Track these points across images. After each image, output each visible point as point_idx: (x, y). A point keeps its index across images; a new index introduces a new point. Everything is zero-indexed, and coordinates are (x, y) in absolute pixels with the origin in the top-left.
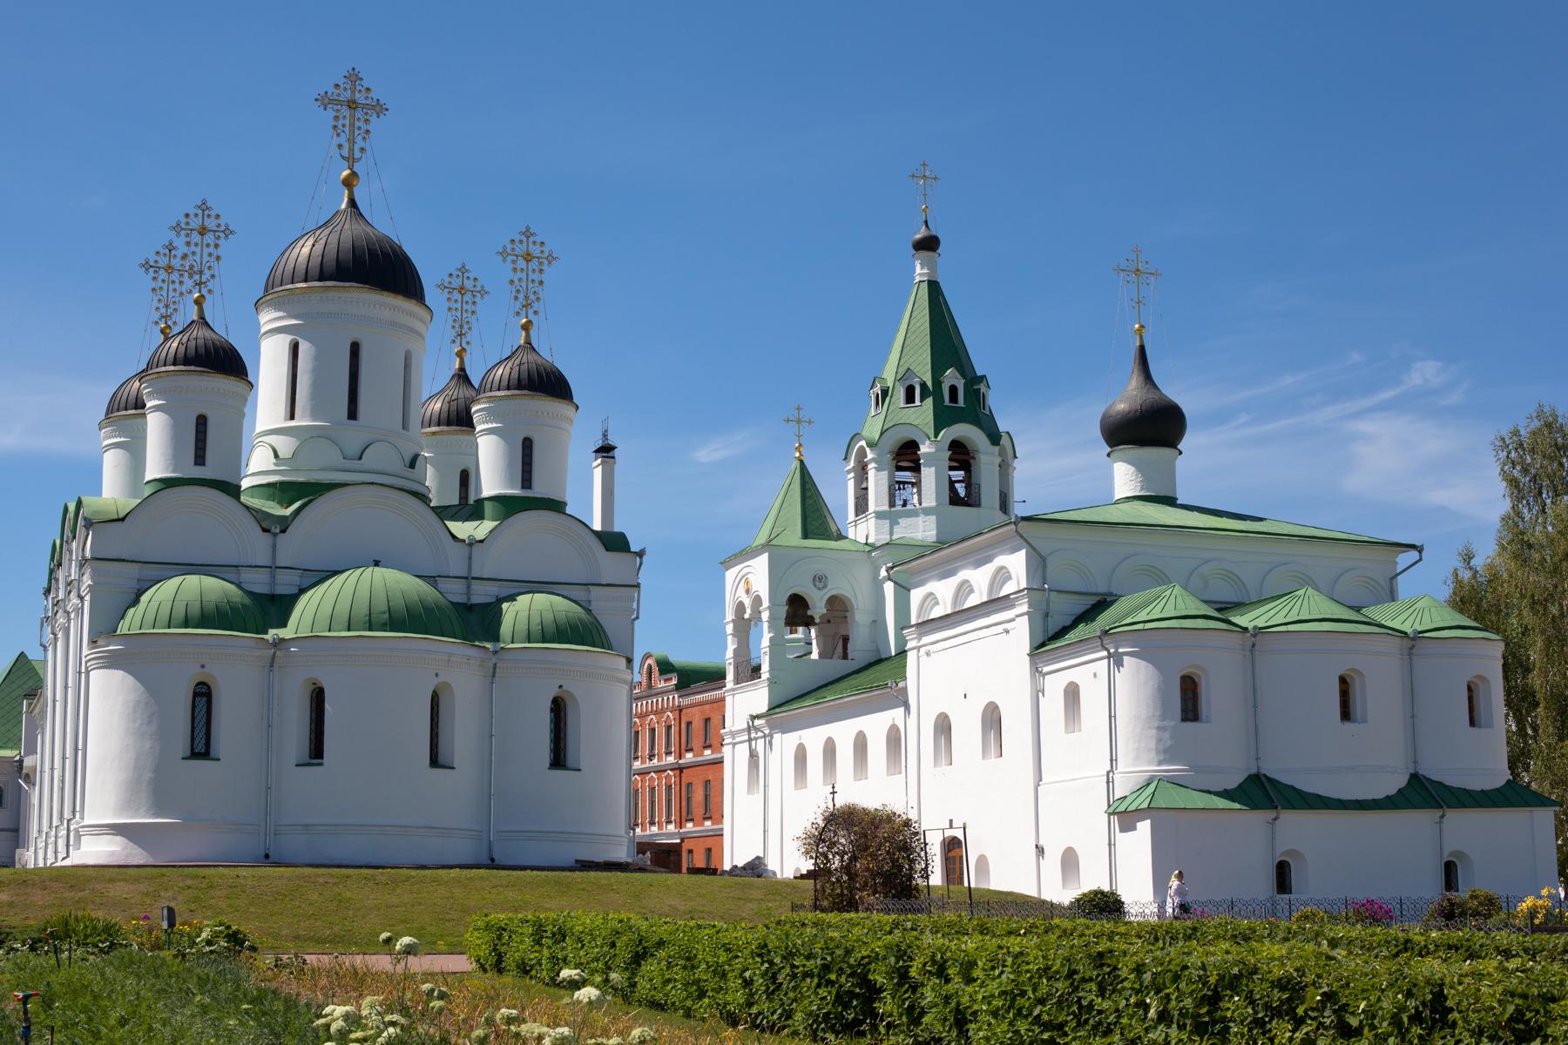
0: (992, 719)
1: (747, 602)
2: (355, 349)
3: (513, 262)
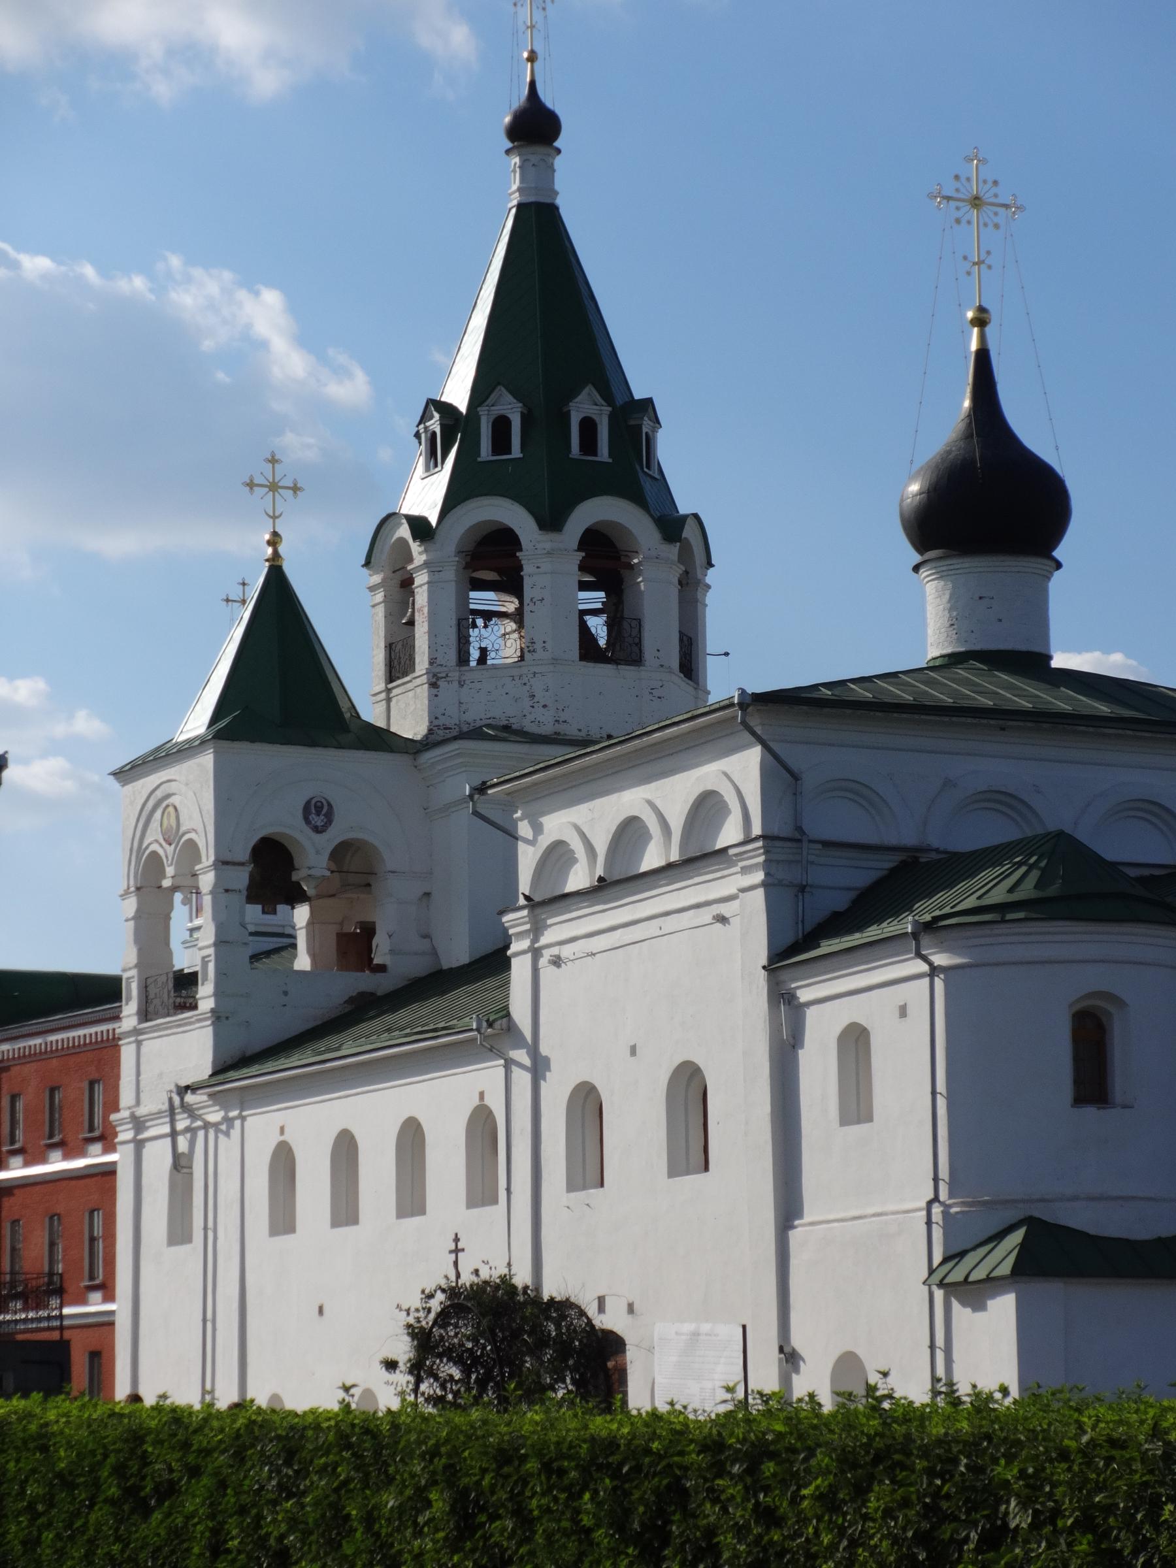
0: (689, 1091)
1: (167, 852)
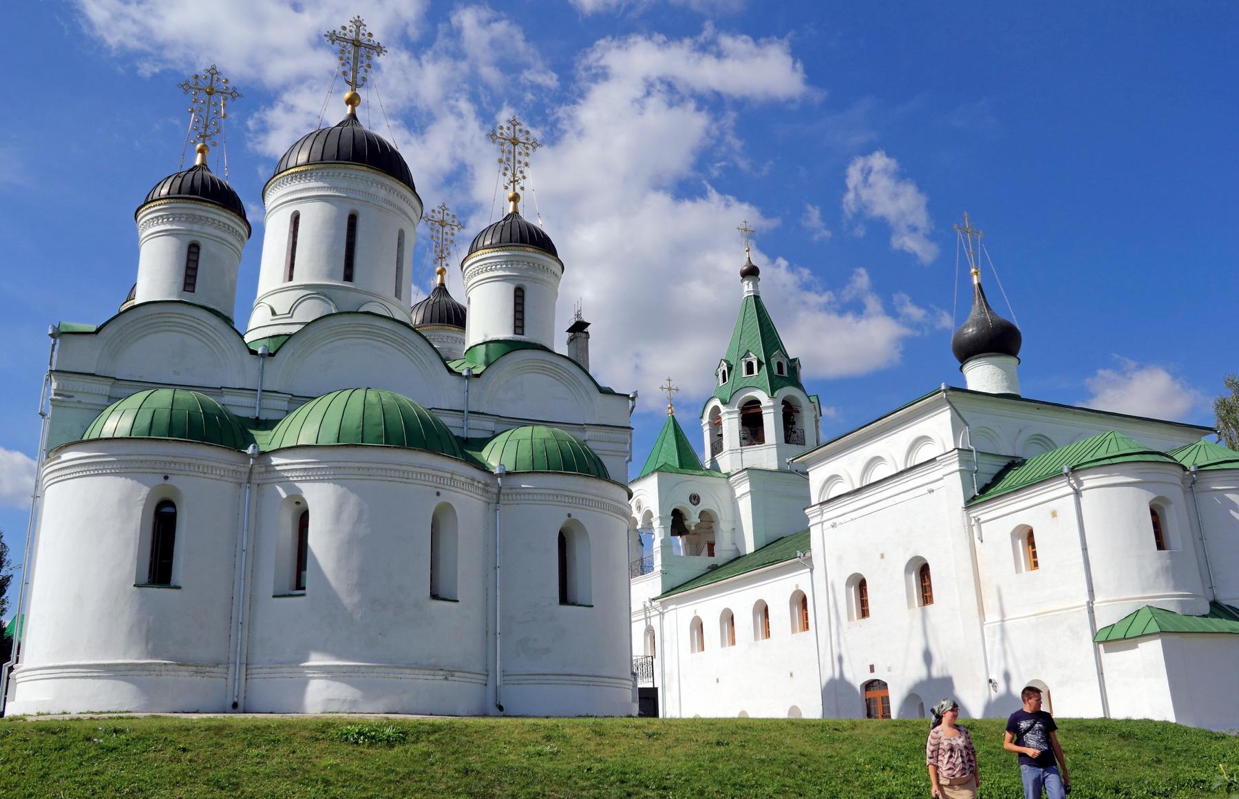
2: (352, 221)
3: (502, 144)
